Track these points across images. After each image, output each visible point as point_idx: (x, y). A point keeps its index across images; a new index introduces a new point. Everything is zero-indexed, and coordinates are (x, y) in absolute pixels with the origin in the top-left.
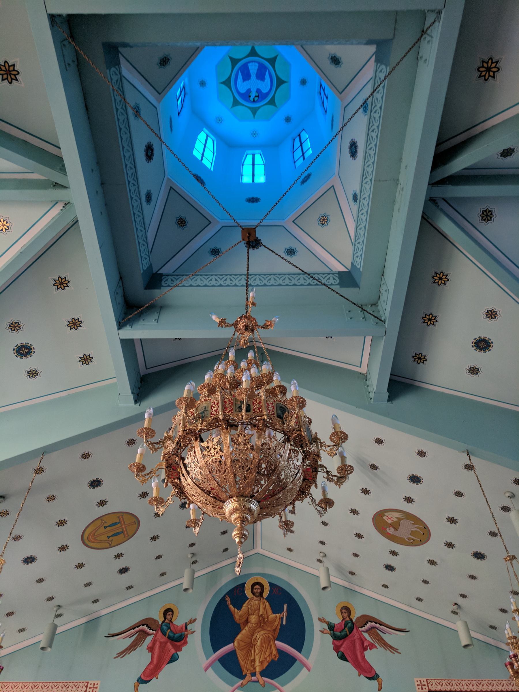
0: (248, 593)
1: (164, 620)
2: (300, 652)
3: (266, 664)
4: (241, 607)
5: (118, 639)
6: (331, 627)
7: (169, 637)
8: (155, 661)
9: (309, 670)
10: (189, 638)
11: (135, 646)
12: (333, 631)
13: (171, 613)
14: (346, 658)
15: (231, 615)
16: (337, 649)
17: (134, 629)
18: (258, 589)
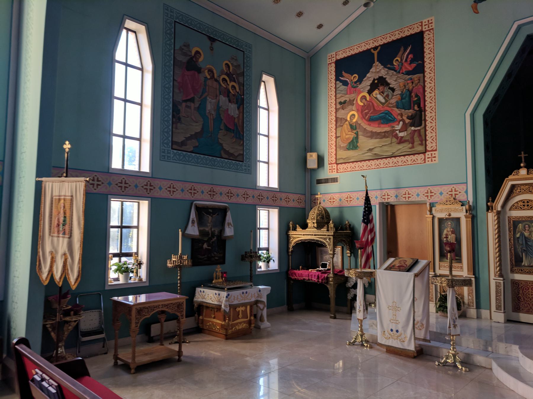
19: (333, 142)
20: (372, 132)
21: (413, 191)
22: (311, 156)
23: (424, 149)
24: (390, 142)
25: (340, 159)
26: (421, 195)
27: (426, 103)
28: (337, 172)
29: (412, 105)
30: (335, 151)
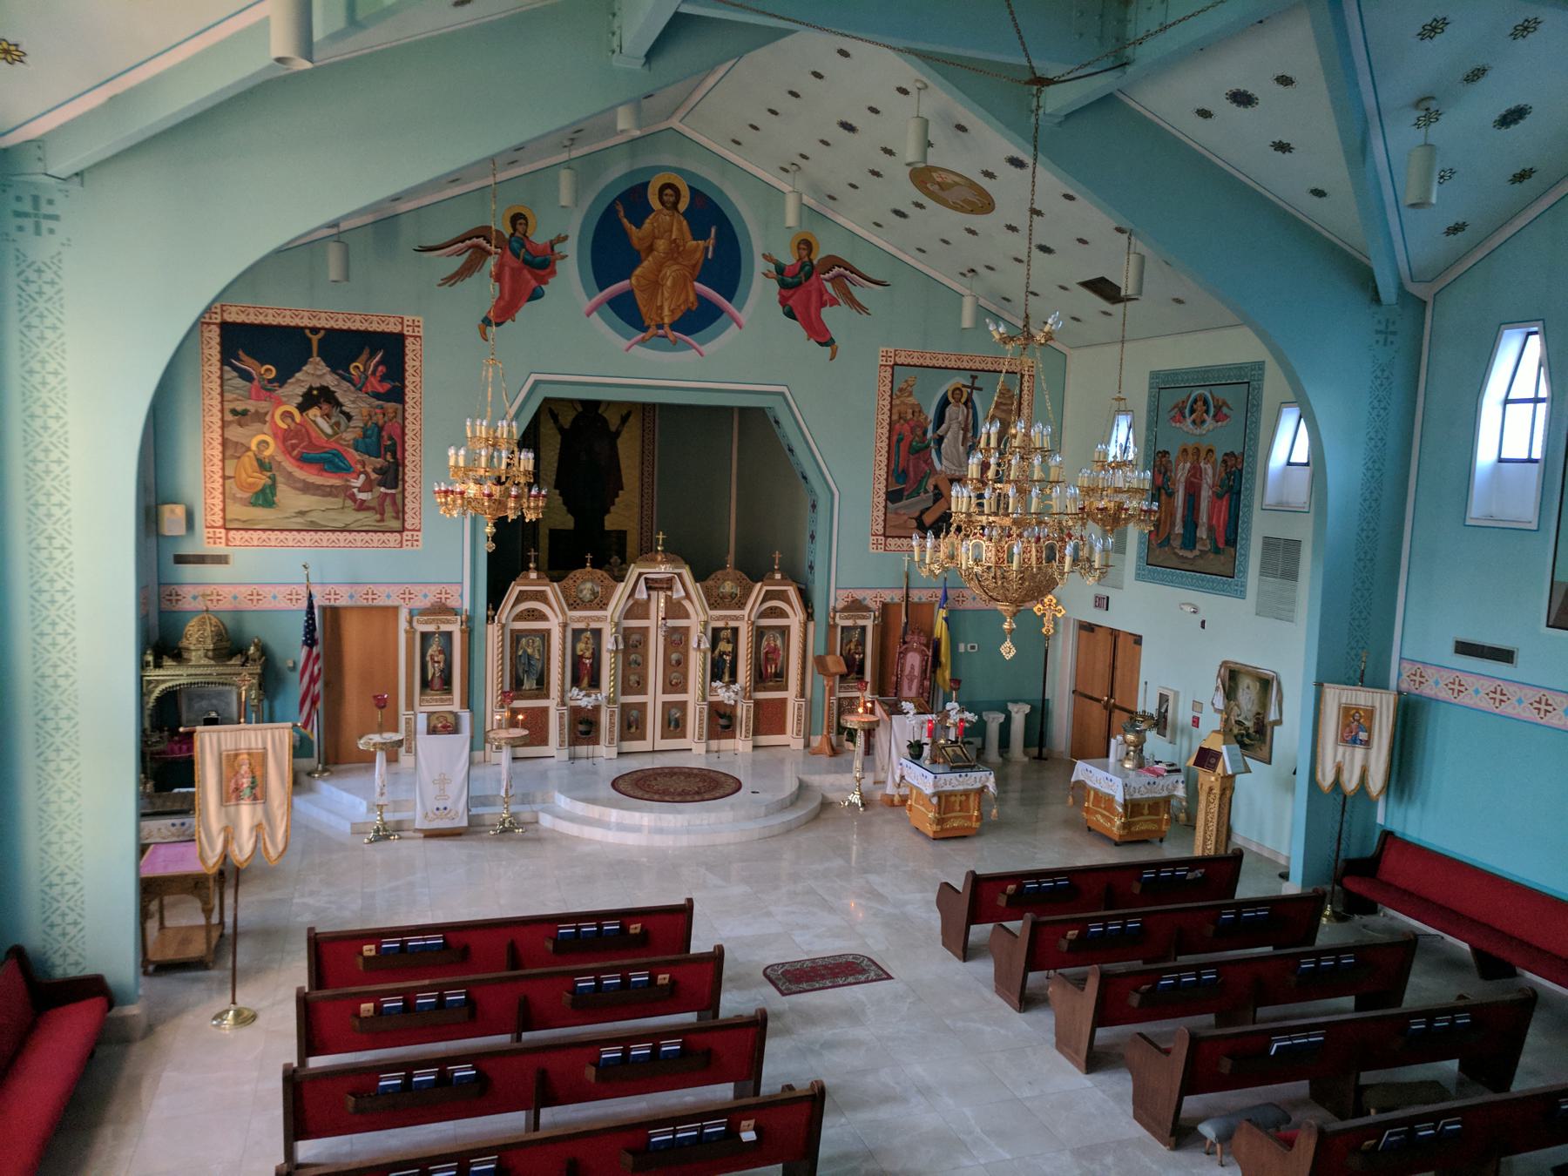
0: (654, 202)
2: (730, 300)
3: (678, 315)
6: (780, 269)
7: (524, 261)
8: (507, 296)
9: (740, 327)
10: (559, 265)
11: (469, 269)
12: (782, 274)
13: (522, 221)
16: (783, 301)
17: (463, 241)
18: (671, 195)
20: (304, 480)
21: (380, 590)
22: (172, 511)
24: (341, 506)
25: (232, 520)
26: (394, 596)
27: (407, 454)
28: (227, 545)
29: (383, 452)
30: (221, 504)
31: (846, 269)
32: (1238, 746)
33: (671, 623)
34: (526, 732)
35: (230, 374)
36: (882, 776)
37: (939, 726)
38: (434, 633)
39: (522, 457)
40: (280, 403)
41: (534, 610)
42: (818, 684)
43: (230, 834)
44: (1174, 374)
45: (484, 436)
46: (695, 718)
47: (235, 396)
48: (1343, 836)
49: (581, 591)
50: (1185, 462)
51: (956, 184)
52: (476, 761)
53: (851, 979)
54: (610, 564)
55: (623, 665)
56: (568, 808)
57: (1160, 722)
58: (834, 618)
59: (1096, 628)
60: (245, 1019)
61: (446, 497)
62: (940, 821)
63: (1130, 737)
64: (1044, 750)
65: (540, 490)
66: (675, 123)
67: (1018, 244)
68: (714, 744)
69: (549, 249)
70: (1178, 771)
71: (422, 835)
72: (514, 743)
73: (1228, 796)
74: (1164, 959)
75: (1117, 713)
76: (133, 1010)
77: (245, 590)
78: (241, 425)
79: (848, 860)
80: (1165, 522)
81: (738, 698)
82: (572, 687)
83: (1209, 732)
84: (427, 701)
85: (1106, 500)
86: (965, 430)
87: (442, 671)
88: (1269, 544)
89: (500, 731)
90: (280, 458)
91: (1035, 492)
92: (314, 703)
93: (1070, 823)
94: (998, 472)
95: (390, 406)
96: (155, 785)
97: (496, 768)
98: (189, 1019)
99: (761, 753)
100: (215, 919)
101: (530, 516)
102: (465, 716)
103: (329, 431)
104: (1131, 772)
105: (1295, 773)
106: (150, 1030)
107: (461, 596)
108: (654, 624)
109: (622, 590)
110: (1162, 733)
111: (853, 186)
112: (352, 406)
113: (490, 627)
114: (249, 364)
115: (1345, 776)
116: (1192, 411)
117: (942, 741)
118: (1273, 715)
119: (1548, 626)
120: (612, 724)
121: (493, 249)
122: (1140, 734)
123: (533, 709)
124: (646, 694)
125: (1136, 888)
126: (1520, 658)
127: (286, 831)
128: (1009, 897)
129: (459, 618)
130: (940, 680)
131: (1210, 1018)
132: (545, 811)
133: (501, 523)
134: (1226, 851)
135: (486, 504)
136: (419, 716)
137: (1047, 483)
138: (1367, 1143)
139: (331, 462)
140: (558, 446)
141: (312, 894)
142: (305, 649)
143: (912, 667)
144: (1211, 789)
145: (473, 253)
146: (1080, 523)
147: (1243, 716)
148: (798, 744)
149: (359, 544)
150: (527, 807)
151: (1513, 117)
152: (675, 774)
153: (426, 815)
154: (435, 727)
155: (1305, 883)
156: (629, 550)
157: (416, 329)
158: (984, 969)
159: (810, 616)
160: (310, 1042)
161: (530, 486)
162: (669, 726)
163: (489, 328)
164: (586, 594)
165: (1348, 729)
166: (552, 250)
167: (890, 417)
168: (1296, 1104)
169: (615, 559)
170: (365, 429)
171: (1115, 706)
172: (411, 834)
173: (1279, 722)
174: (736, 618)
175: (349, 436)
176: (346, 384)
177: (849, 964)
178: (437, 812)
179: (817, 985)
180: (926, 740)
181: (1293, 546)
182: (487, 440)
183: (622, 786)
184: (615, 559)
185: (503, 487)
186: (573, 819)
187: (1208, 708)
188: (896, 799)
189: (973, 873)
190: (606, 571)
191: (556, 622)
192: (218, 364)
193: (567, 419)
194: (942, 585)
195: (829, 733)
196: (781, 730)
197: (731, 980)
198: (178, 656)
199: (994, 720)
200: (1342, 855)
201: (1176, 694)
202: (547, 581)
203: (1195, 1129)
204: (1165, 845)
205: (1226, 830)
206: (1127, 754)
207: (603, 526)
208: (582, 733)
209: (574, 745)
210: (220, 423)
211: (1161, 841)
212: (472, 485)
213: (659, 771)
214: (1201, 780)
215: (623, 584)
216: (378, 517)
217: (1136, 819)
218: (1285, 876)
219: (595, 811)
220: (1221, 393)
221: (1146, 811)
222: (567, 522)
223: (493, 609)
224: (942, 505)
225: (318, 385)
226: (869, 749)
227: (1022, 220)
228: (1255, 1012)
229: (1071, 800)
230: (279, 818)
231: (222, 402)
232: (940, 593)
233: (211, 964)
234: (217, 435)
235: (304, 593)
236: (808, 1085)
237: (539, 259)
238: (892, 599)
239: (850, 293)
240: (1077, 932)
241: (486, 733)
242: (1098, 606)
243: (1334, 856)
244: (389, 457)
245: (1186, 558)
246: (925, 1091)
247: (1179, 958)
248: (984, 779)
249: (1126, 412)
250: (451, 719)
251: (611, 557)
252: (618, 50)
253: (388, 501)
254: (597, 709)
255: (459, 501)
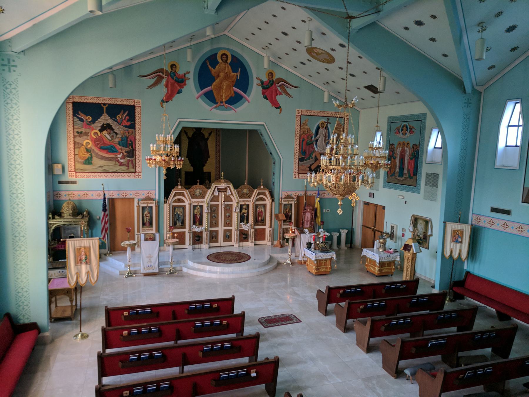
0: (219, 60)
1: (171, 70)
2: (245, 93)
3: (228, 98)
4: (215, 67)
5: (147, 79)
6: (262, 83)
7: (176, 81)
8: (170, 92)
9: (249, 102)
10: (187, 82)
13: (175, 67)
14: (267, 98)
15: (210, 71)
16: (263, 94)
17: (154, 74)
19: (72, 157)
20: (102, 156)
21: (127, 192)
22: (57, 166)
23: (135, 171)
24: (114, 164)
25: (78, 169)
30: (74, 164)
31: (285, 82)
32: (417, 243)
33: (226, 203)
34: (178, 240)
35: (76, 119)
36: (298, 254)
37: (317, 237)
38: (146, 207)
39: (175, 147)
40: (93, 129)
41: (180, 199)
42: (276, 224)
43: (78, 275)
44: (396, 117)
45: (162, 140)
46: (235, 235)
47: (78, 127)
48: (453, 273)
49: (196, 193)
50: (400, 147)
51: (322, 53)
52: (161, 250)
53: (288, 322)
54: (205, 183)
55: (210, 217)
56: (192, 265)
57: (391, 236)
58: (281, 201)
59: (370, 204)
60: (84, 337)
61: (150, 161)
62: (317, 269)
63: (381, 241)
64: (352, 245)
65: (181, 158)
66: (226, 33)
67: (343, 74)
68: (241, 244)
69: (184, 77)
70: (398, 252)
71: (143, 275)
72: (174, 244)
73: (414, 260)
74: (393, 315)
75: (377, 232)
76: (47, 334)
77: (83, 193)
78: (80, 137)
79: (286, 283)
80: (393, 168)
81: (249, 228)
82: (193, 225)
83: (408, 239)
84: (144, 230)
85: (373, 160)
86: (325, 137)
87: (149, 220)
88: (428, 175)
89: (169, 240)
90: (93, 148)
91: (349, 158)
92: (106, 231)
93: (362, 270)
94: (336, 151)
95: (130, 130)
96: (53, 259)
97: (168, 252)
98: (65, 337)
99: (257, 247)
100: (74, 304)
101: (178, 167)
102: (157, 235)
103: (110, 139)
104: (382, 252)
105: (437, 252)
106: (52, 341)
107: (155, 194)
108: (221, 203)
109: (209, 192)
110: (392, 239)
111: (287, 54)
112: (117, 130)
113: (165, 205)
114: (82, 116)
115: (454, 253)
116: (402, 130)
117: (318, 242)
118: (429, 233)
119: (522, 202)
120: (207, 237)
121: (164, 76)
122: (385, 240)
123: (180, 232)
124: (218, 227)
125: (383, 291)
126: (513, 213)
127: (97, 274)
128: (341, 294)
129: (155, 202)
130: (317, 222)
131: (408, 335)
132: (184, 267)
133: (168, 169)
134: (414, 278)
135: (163, 163)
136: (142, 234)
137: (353, 155)
138: (461, 376)
139: (111, 149)
140: (188, 143)
141: (106, 295)
142: (103, 213)
143: (308, 217)
144: (408, 258)
145: (158, 77)
146: (364, 168)
147: (419, 233)
148: (269, 243)
149: (121, 177)
150: (178, 265)
151: (511, 29)
152: (228, 254)
153: (144, 268)
154: (147, 239)
155: (440, 290)
156: (212, 178)
157: (139, 104)
158: (332, 318)
159: (273, 200)
160: (106, 344)
161: (178, 157)
162: (226, 238)
163: (163, 103)
164: (198, 194)
165: (454, 238)
166: (185, 76)
167: (300, 133)
168: (438, 363)
169: (207, 182)
170: (122, 138)
171: (376, 230)
172: (139, 274)
173: (431, 235)
174: (248, 201)
175: (117, 140)
176: (115, 123)
177: (287, 317)
178: (148, 267)
179: (276, 324)
180: (312, 242)
181: (436, 176)
182: (163, 141)
183: (210, 258)
184: (207, 182)
185: (169, 157)
186: (194, 269)
187: (407, 231)
188: (303, 262)
189: (328, 286)
190: (204, 186)
191: (188, 203)
192: (72, 116)
193: (190, 134)
194: (317, 190)
195: (280, 240)
196: (264, 239)
197: (247, 323)
198: (60, 215)
199: (335, 235)
200: (453, 280)
201: (397, 226)
202: (184, 189)
203: (403, 371)
204: (393, 277)
205: (414, 272)
206: (380, 246)
207: (203, 170)
208: (197, 240)
209: (194, 244)
210: (73, 136)
211: (392, 275)
212: (158, 157)
213: (223, 253)
214: (405, 255)
215: (210, 190)
216: (127, 168)
217: (383, 268)
218: (433, 287)
219: (201, 266)
220: (412, 124)
221: (386, 265)
222: (191, 169)
223: (166, 199)
224: (317, 162)
225: (106, 123)
226: (293, 245)
227: (344, 66)
228: (423, 332)
229: (361, 262)
230: (95, 269)
231: (73, 129)
232: (317, 192)
233: (73, 319)
234: (72, 140)
235: (102, 194)
236: (274, 358)
237: (180, 80)
238: (301, 194)
239: (286, 90)
240: (363, 306)
241: (164, 240)
242: (370, 196)
243: (450, 280)
244: (130, 147)
245: (400, 180)
246: (312, 359)
247: (398, 315)
248: (332, 255)
249: (380, 130)
250: (152, 236)
251: (206, 181)
252: (206, 7)
253: (130, 163)
254: (202, 232)
255: (154, 162)
